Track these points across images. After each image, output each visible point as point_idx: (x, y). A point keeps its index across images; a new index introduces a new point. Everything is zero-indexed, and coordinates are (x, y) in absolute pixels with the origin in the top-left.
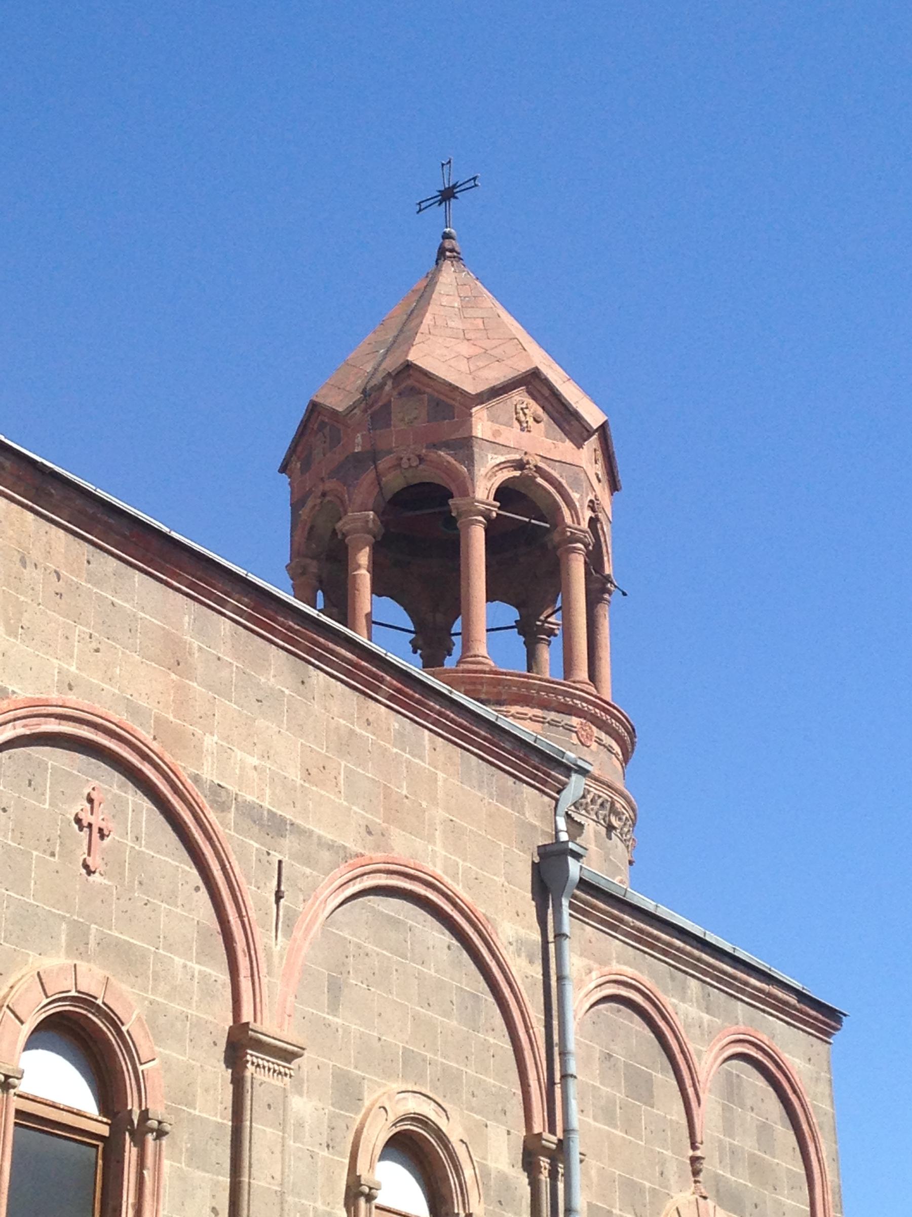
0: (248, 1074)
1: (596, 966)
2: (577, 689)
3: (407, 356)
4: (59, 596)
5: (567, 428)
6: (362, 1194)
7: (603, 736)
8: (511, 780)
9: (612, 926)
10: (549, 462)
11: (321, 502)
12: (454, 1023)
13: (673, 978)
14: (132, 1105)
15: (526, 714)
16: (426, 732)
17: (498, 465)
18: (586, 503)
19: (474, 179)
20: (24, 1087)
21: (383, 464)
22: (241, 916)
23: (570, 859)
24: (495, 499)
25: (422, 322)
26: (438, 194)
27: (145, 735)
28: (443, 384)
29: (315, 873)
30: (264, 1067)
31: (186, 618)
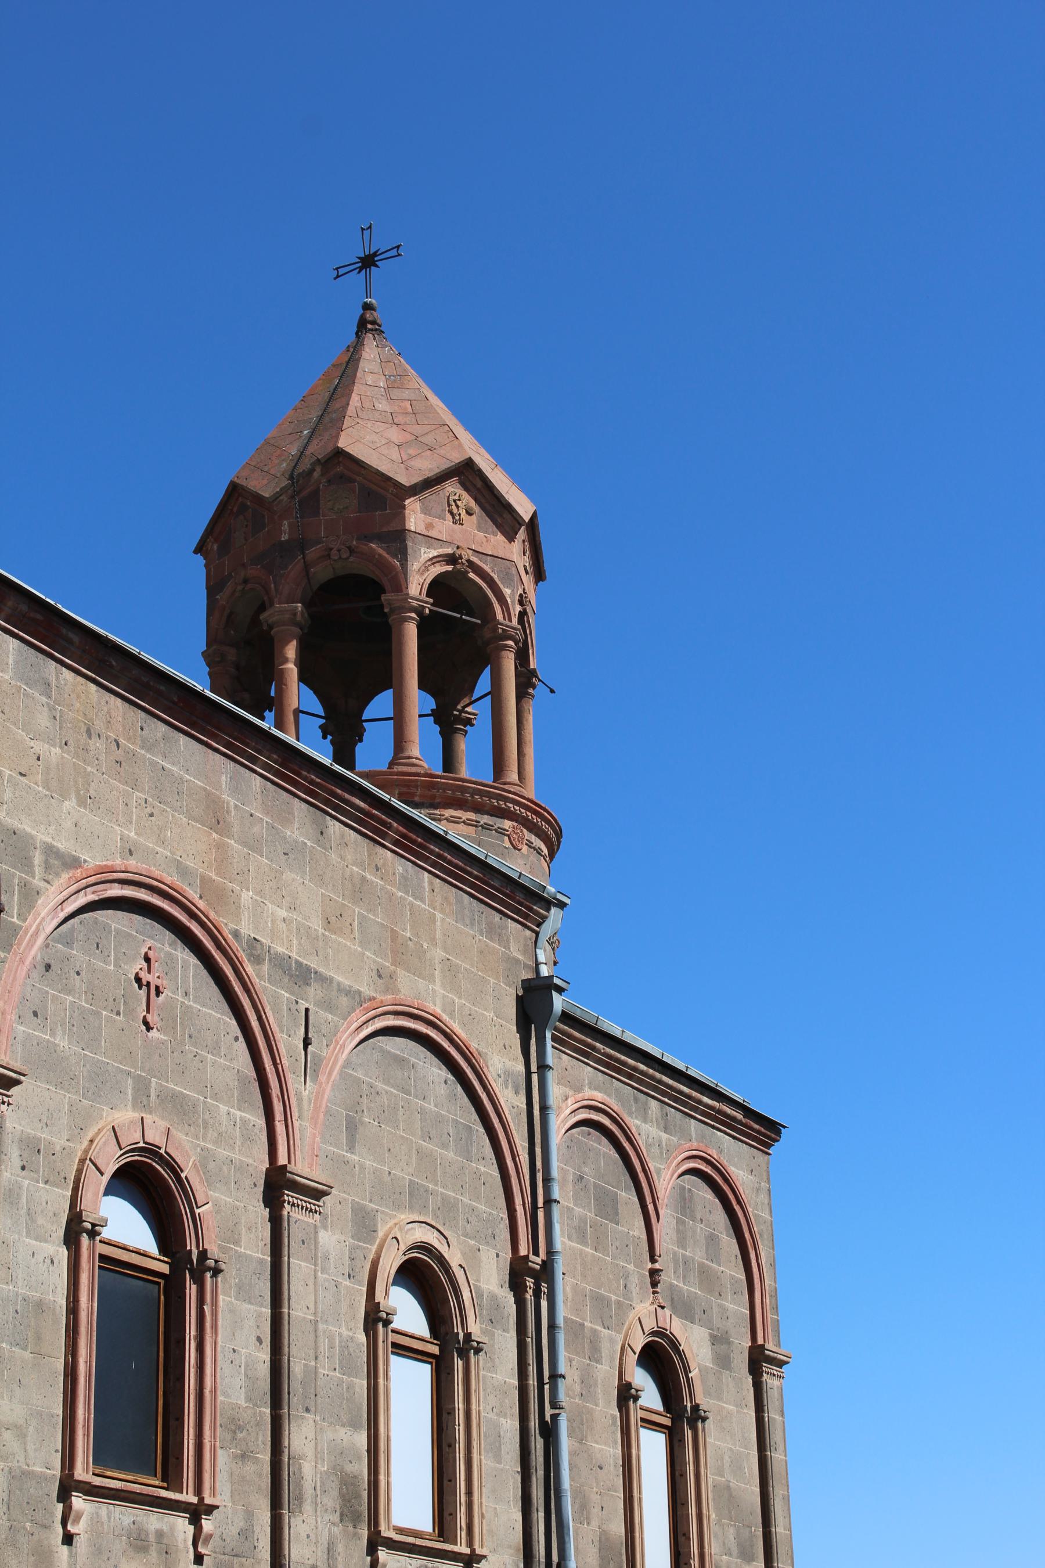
0: (285, 1213)
1: (571, 1093)
2: (510, 792)
3: (337, 441)
4: (119, 764)
5: (499, 520)
6: (380, 1319)
7: (533, 838)
8: (497, 917)
9: (585, 1054)
10: (481, 555)
11: (244, 588)
12: (451, 1155)
13: (636, 1100)
14: (191, 1245)
15: (460, 818)
16: (426, 874)
17: (431, 559)
18: (517, 598)
19: (398, 247)
20: (106, 1233)
21: (312, 553)
22: (275, 1064)
23: (555, 994)
24: (428, 596)
25: (348, 404)
27: (193, 894)
28: (376, 473)
29: (336, 1019)
30: (298, 1206)
31: (224, 778)
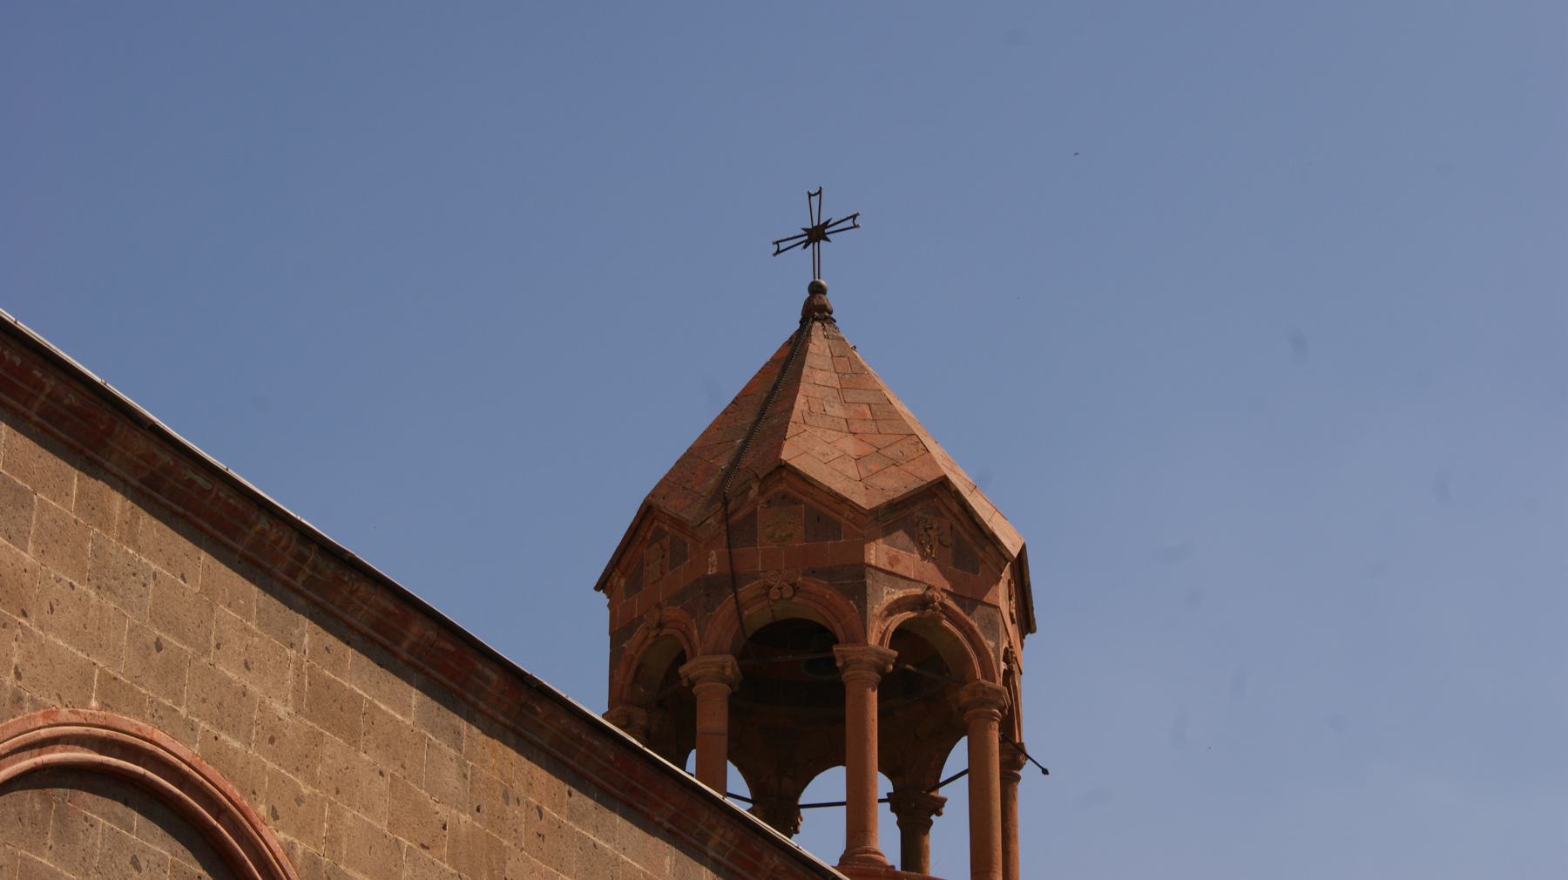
3: (779, 452)
4: (541, 838)
11: (658, 635)
21: (747, 591)
24: (891, 647)
25: (793, 408)
26: (804, 232)
28: (828, 494)
31: (668, 860)
